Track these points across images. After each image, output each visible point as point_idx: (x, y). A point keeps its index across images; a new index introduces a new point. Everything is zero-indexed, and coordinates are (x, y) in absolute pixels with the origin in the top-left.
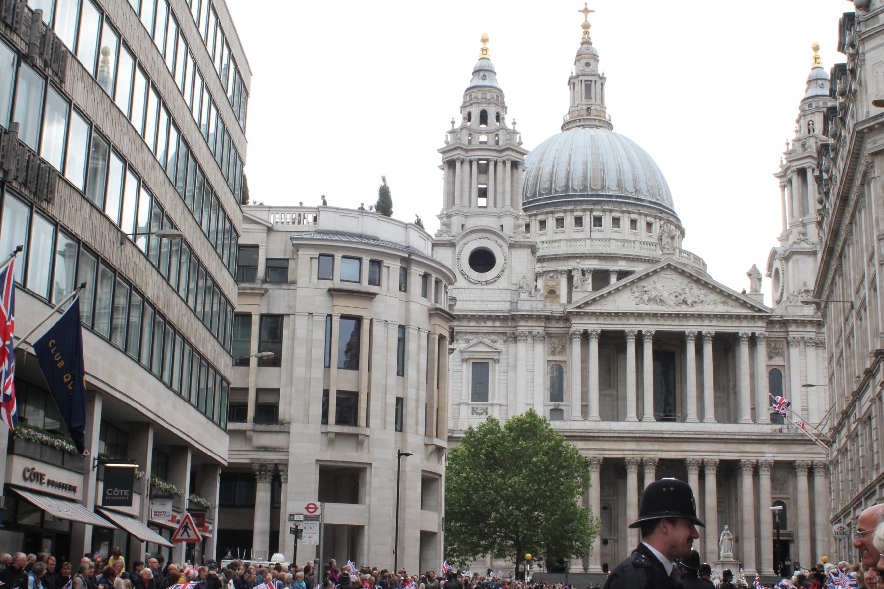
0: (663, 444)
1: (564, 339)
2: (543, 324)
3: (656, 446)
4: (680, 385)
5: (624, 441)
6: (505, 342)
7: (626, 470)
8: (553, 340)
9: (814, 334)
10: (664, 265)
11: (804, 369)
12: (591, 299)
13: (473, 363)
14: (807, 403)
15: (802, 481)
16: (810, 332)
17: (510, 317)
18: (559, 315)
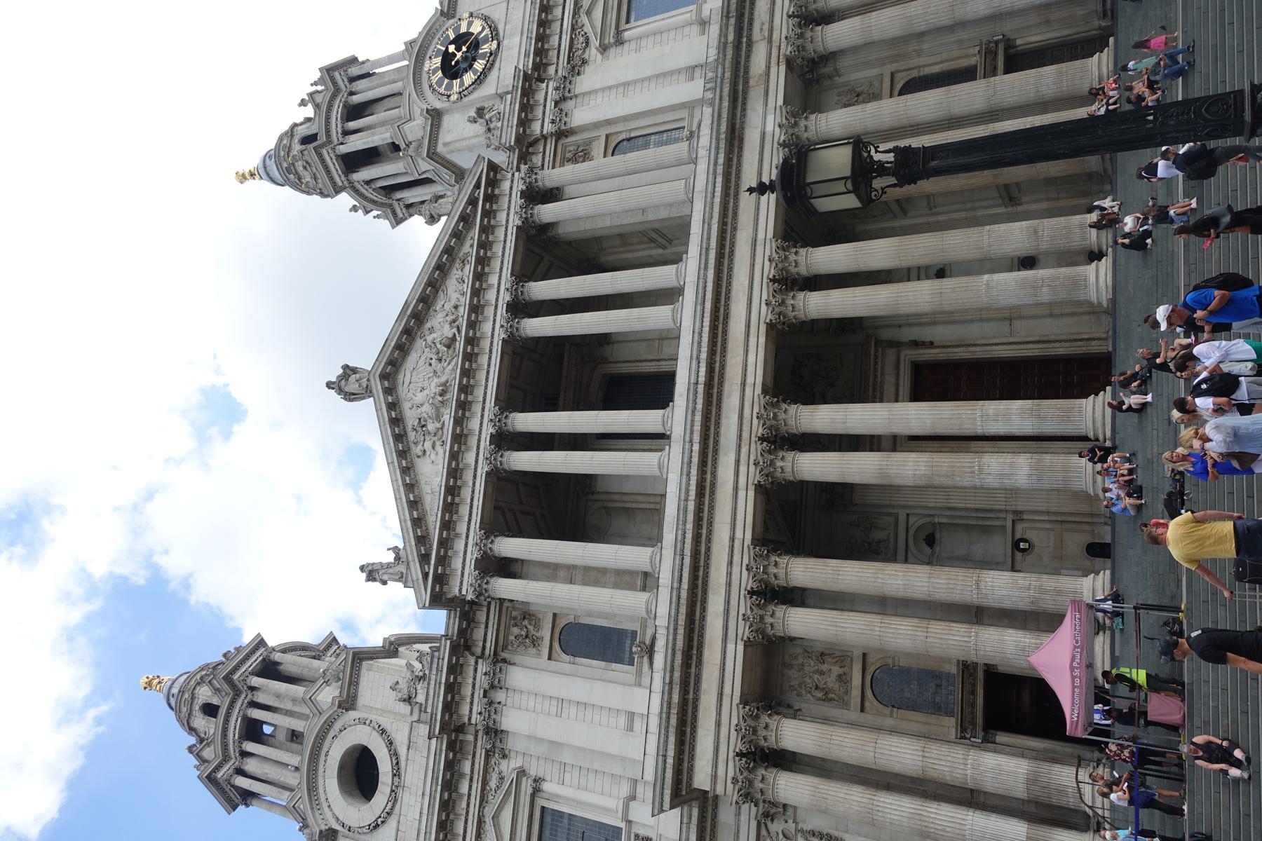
1: (514, 614)
2: (472, 660)
3: (731, 402)
4: (661, 363)
5: (713, 485)
6: (504, 756)
7: (791, 482)
8: (512, 638)
9: (551, 83)
11: (613, 92)
12: (414, 548)
14: (679, 71)
15: (837, 35)
16: (547, 92)
17: (454, 734)
18: (457, 620)
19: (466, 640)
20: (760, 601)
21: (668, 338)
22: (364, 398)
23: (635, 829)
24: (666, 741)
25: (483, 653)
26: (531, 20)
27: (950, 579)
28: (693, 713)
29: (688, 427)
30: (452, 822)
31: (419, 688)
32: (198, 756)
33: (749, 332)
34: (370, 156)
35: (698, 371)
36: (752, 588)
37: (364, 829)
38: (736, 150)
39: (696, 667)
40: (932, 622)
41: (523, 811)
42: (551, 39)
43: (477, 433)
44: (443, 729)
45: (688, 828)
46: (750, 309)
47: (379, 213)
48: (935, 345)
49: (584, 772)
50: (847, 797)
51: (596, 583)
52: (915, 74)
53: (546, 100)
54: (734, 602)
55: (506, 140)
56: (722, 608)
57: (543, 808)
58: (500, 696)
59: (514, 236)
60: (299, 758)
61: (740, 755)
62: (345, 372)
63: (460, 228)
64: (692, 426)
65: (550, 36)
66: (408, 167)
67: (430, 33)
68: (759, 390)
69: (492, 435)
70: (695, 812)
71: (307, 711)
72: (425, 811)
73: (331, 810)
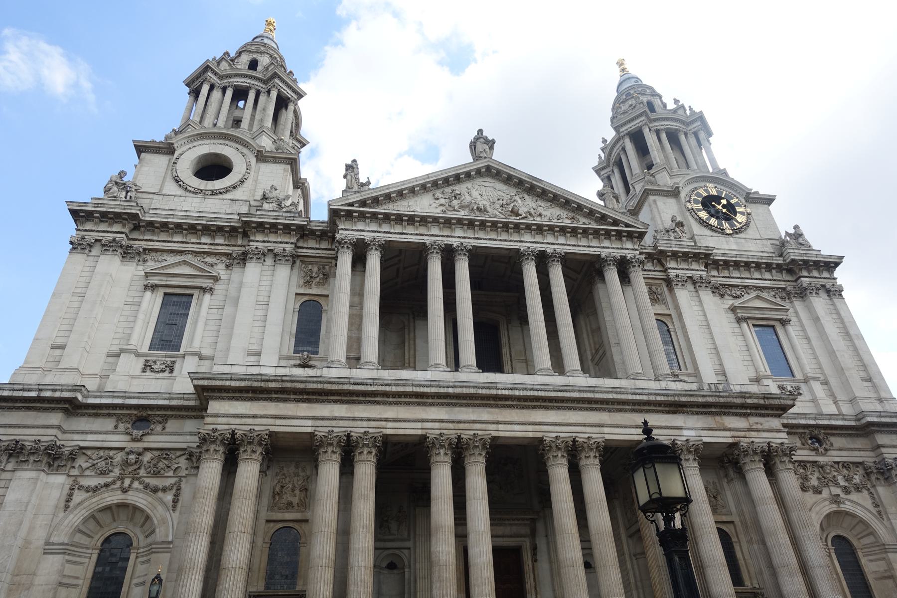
0: (496, 410)
1: (327, 267)
2: (293, 240)
3: (484, 414)
4: (509, 362)
5: (424, 404)
6: (227, 266)
7: (429, 460)
8: (310, 267)
10: (480, 166)
11: (702, 318)
12: (370, 196)
13: (165, 294)
14: (721, 364)
15: (758, 479)
16: (698, 270)
17: (242, 230)
18: (321, 228)
19: (307, 235)
20: (343, 443)
21: (527, 365)
22: (472, 155)
23: (179, 361)
24: (241, 380)
25: (299, 247)
26: (749, 257)
27: (364, 582)
28: (262, 398)
29: (465, 384)
30: (181, 233)
31: (273, 204)
32: (222, 59)
33: (536, 424)
34: (642, 149)
35: (505, 389)
36: (352, 436)
37: (175, 173)
38: (667, 409)
39: (295, 399)
40: (333, 570)
41: (189, 282)
42: (737, 272)
43: (453, 235)
44: (245, 223)
45: (181, 399)
46: (553, 425)
47: (603, 158)
48: (535, 563)
49: (218, 322)
50: (205, 513)
51: (351, 324)
52: (734, 539)
53: (693, 270)
54: (341, 423)
55: (661, 243)
56: (337, 415)
57: (192, 295)
58: (269, 261)
59: (593, 253)
60: (222, 126)
61: (233, 433)
62: (490, 141)
63: (597, 215)
64: (466, 387)
65: (739, 270)
66: (637, 176)
67: (734, 186)
68: (494, 434)
69: (451, 245)
70: (192, 403)
71: (254, 130)
72: (188, 214)
73: (187, 150)
